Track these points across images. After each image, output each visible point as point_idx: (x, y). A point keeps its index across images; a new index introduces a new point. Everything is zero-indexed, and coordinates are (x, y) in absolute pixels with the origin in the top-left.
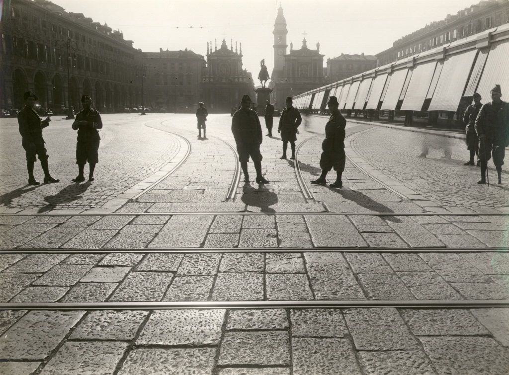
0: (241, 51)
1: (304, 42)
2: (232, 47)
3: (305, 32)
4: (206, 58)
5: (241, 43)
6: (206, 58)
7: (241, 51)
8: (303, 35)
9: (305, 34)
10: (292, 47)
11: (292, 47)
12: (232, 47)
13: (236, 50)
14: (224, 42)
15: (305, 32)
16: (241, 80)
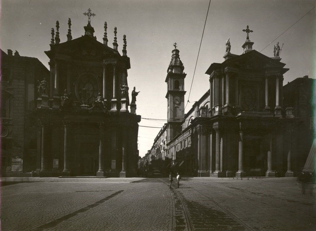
0: (125, 51)
1: (249, 44)
2: (105, 39)
3: (248, 27)
4: (45, 61)
5: (125, 36)
6: (45, 61)
7: (125, 51)
8: (245, 33)
9: (248, 31)
10: (229, 49)
11: (229, 49)
12: (105, 39)
13: (115, 44)
14: (89, 29)
15: (248, 27)
16: (123, 108)
